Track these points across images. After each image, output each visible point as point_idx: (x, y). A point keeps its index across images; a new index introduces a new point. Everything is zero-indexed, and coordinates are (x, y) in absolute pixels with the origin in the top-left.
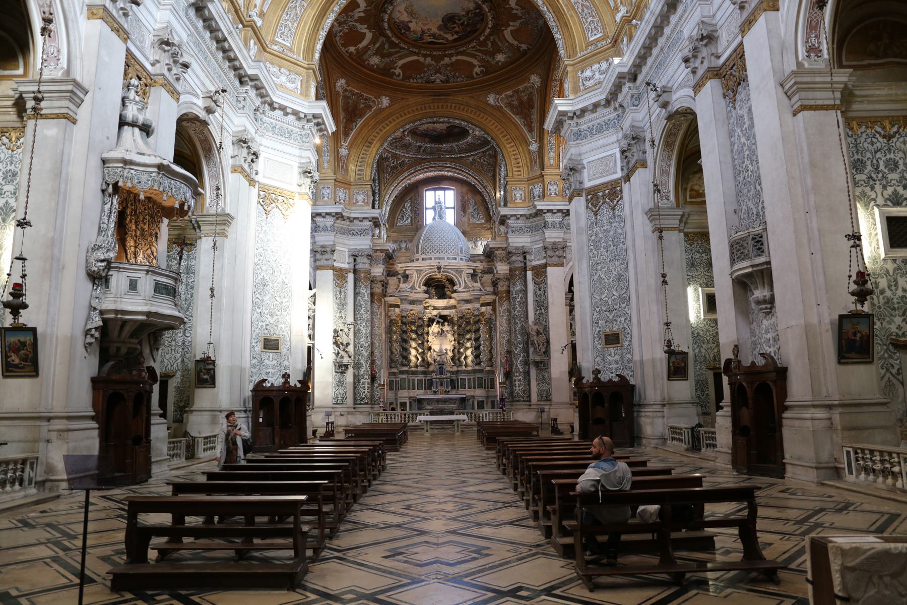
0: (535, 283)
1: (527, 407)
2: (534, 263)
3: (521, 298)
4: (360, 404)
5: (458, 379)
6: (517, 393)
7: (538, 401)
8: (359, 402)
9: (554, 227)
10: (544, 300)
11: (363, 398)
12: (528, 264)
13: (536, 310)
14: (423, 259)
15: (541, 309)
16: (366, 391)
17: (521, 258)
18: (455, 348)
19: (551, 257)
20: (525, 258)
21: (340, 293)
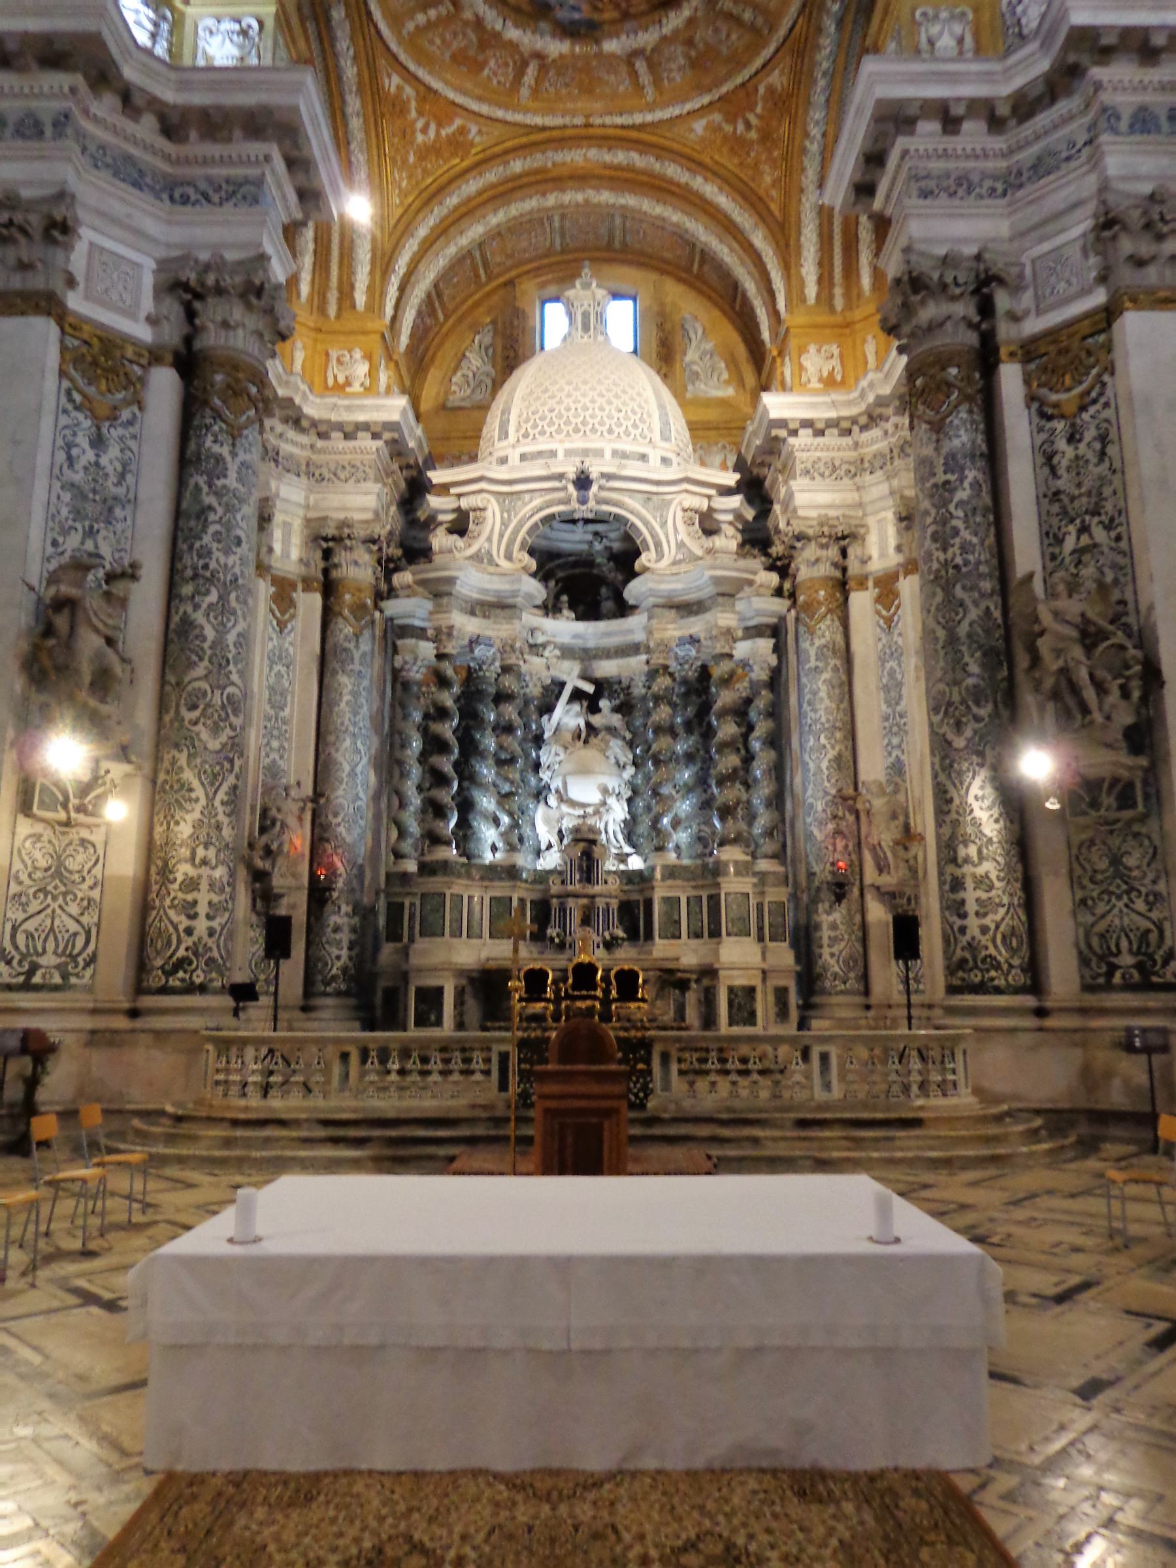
0: (1044, 413)
1: (1031, 1022)
2: (1033, 326)
3: (976, 484)
4: (164, 990)
5: (649, 903)
6: (971, 947)
7: (1088, 988)
8: (156, 979)
9: (1145, 130)
10: (1102, 481)
11: (181, 964)
12: (1005, 331)
13: (1051, 538)
14: (523, 457)
15: (1084, 529)
16: (201, 925)
17: (965, 309)
18: (635, 791)
19: (1139, 263)
20: (986, 308)
21: (98, 442)
